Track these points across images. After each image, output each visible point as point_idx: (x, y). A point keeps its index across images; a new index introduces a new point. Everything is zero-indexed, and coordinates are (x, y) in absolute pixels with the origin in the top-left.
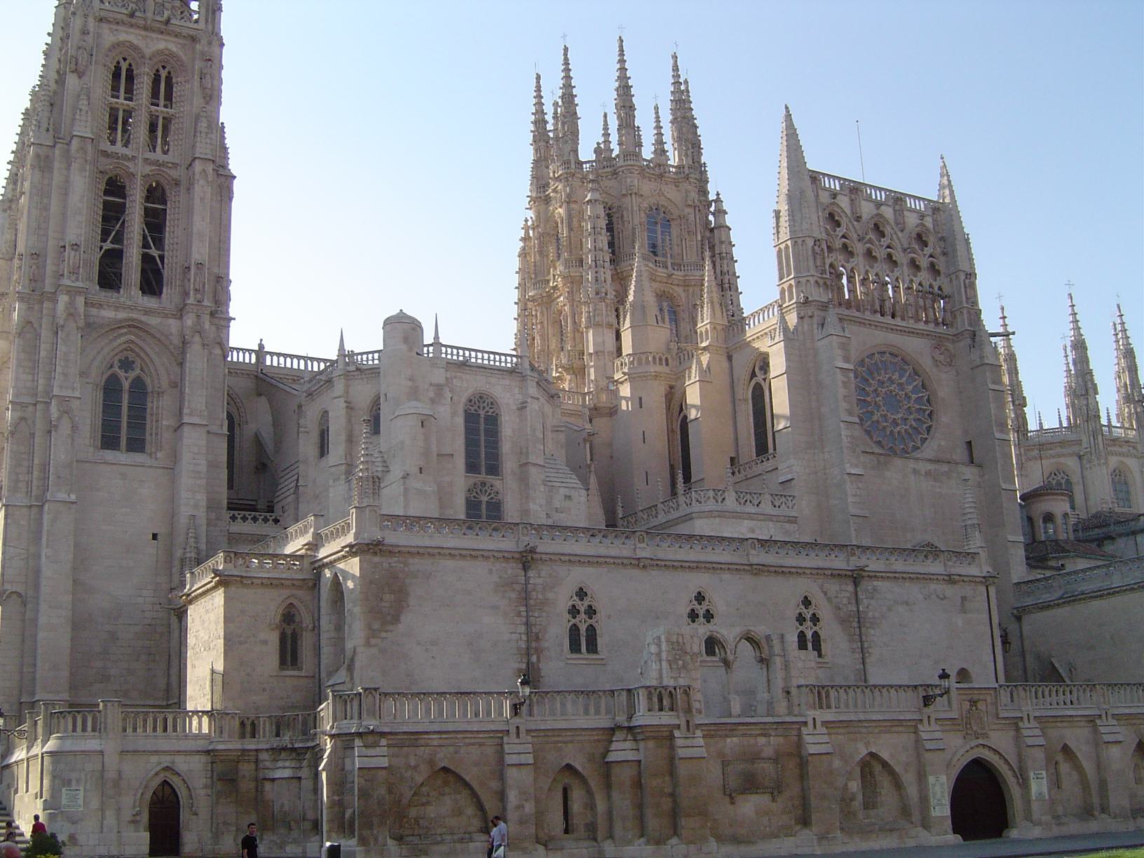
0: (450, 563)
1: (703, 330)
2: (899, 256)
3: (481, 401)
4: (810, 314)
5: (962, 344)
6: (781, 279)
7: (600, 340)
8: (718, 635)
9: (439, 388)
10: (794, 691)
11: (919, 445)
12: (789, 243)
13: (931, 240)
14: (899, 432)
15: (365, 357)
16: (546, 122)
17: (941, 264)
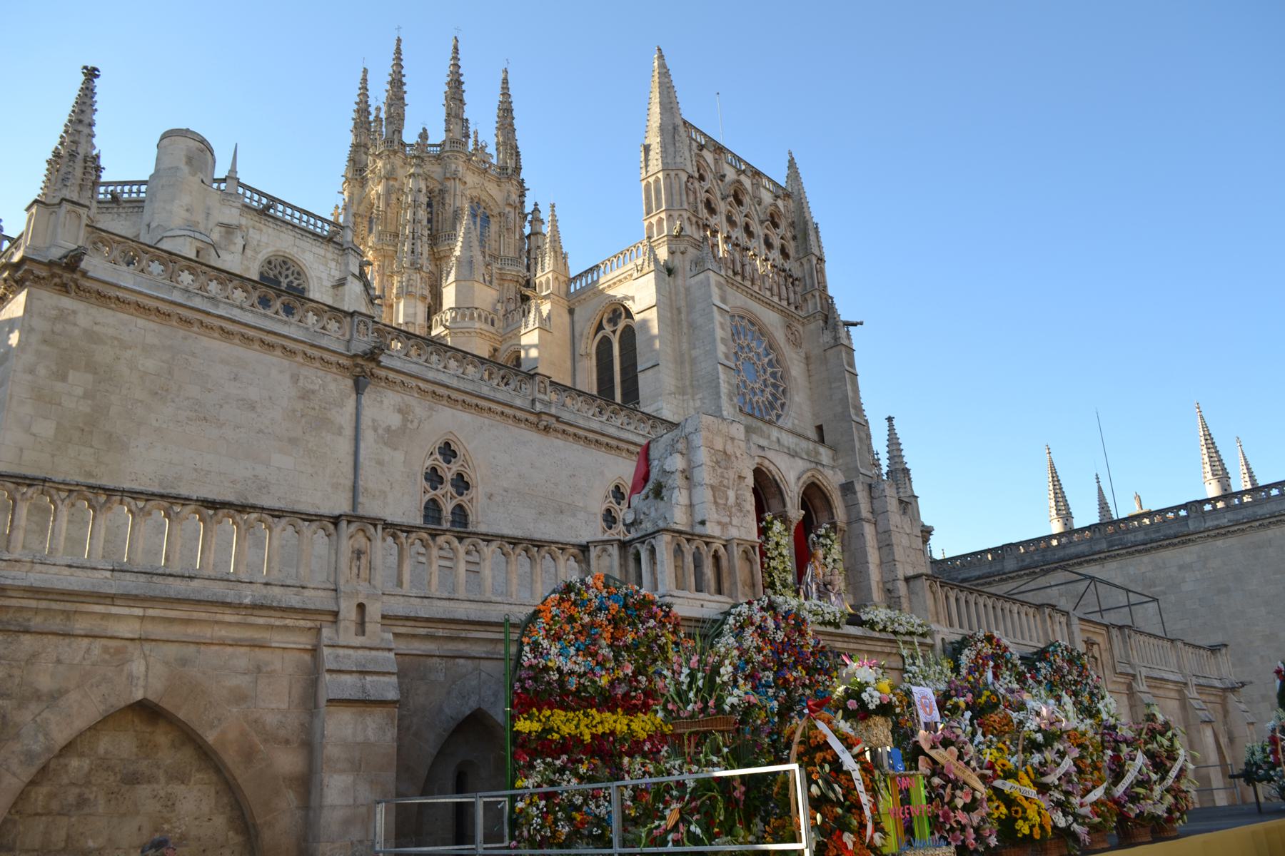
0: (220, 347)
1: (543, 279)
2: (755, 227)
3: (285, 267)
4: (682, 249)
5: (812, 326)
6: (649, 212)
7: (411, 311)
8: (772, 468)
9: (229, 229)
10: (902, 587)
11: (774, 419)
12: (660, 175)
13: (783, 223)
14: (757, 402)
15: (126, 189)
16: (369, 113)
17: (791, 247)
